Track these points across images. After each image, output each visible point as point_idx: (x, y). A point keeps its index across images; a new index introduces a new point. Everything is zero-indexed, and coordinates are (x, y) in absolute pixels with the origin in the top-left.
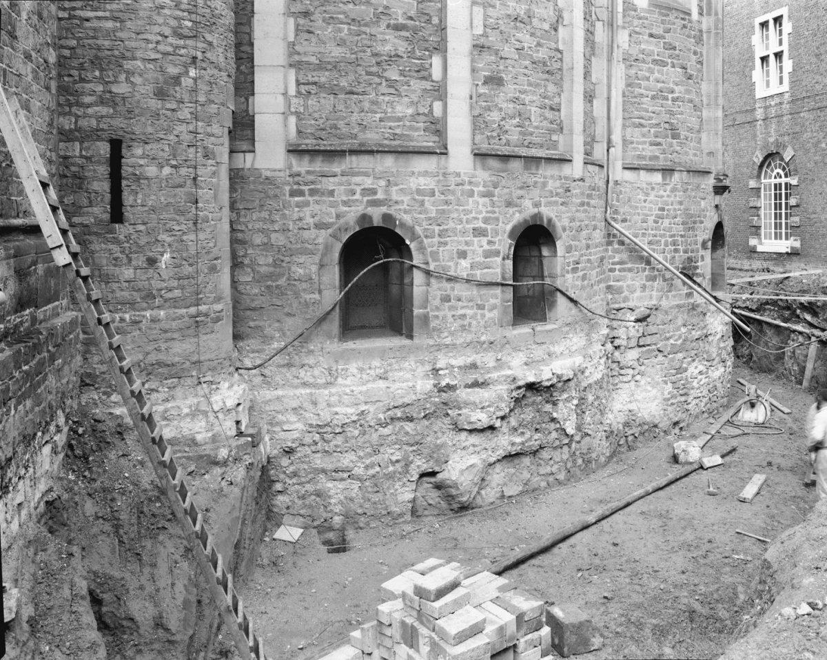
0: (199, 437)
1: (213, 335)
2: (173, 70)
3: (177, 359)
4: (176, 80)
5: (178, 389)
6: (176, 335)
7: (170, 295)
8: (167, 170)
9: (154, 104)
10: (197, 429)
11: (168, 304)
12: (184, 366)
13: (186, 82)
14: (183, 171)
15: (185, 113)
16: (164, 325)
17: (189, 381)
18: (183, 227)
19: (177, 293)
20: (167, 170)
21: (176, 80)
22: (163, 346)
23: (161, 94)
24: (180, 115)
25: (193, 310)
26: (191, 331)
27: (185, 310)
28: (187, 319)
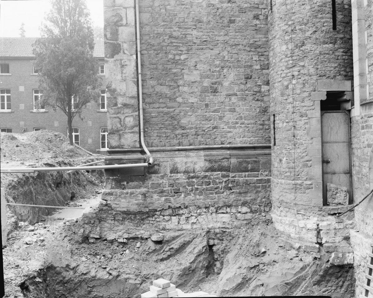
0: (292, 235)
1: (304, 195)
2: (286, 83)
3: (288, 201)
4: (287, 87)
5: (289, 213)
6: (287, 191)
7: (286, 175)
8: (285, 124)
9: (280, 98)
10: (291, 231)
11: (285, 178)
12: (291, 204)
13: (290, 87)
14: (291, 124)
15: (290, 100)
16: (284, 186)
17: (292, 211)
18: (290, 147)
19: (288, 174)
20: (285, 124)
21: (287, 87)
22: (284, 194)
23: (282, 95)
24: (289, 101)
25: (293, 182)
26: (293, 191)
27: (291, 181)
28: (291, 185)
